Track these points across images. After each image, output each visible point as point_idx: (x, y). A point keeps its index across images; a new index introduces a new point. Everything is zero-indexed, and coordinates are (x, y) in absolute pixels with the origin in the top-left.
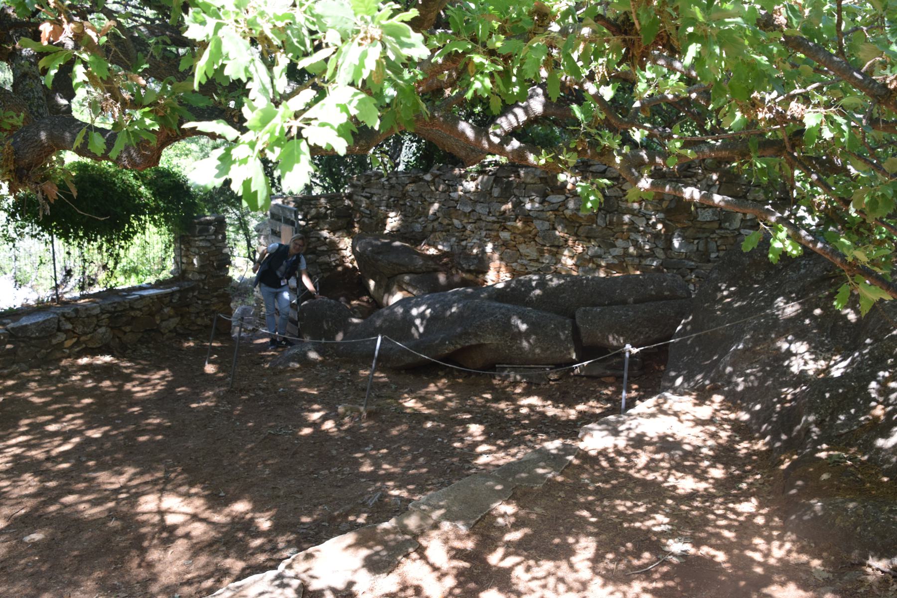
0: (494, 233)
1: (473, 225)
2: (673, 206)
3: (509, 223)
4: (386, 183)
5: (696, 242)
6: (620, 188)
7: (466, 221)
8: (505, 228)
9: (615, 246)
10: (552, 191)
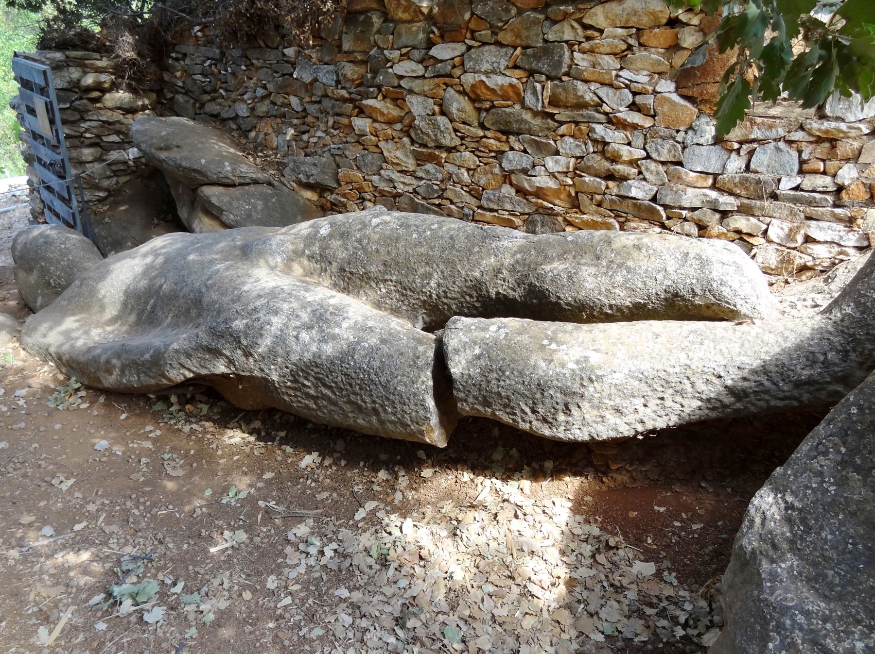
0: (345, 121)
1: (317, 106)
2: (699, 61)
3: (364, 102)
4: (199, 34)
6: (579, 21)
7: (307, 99)
8: (361, 112)
10: (442, 36)
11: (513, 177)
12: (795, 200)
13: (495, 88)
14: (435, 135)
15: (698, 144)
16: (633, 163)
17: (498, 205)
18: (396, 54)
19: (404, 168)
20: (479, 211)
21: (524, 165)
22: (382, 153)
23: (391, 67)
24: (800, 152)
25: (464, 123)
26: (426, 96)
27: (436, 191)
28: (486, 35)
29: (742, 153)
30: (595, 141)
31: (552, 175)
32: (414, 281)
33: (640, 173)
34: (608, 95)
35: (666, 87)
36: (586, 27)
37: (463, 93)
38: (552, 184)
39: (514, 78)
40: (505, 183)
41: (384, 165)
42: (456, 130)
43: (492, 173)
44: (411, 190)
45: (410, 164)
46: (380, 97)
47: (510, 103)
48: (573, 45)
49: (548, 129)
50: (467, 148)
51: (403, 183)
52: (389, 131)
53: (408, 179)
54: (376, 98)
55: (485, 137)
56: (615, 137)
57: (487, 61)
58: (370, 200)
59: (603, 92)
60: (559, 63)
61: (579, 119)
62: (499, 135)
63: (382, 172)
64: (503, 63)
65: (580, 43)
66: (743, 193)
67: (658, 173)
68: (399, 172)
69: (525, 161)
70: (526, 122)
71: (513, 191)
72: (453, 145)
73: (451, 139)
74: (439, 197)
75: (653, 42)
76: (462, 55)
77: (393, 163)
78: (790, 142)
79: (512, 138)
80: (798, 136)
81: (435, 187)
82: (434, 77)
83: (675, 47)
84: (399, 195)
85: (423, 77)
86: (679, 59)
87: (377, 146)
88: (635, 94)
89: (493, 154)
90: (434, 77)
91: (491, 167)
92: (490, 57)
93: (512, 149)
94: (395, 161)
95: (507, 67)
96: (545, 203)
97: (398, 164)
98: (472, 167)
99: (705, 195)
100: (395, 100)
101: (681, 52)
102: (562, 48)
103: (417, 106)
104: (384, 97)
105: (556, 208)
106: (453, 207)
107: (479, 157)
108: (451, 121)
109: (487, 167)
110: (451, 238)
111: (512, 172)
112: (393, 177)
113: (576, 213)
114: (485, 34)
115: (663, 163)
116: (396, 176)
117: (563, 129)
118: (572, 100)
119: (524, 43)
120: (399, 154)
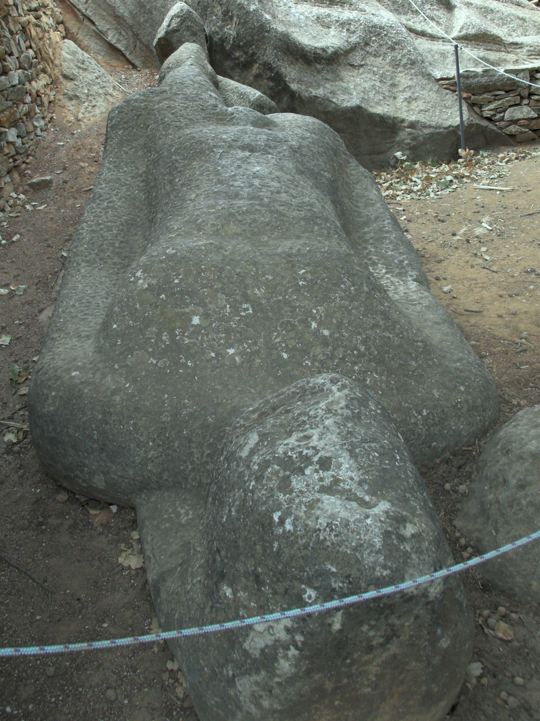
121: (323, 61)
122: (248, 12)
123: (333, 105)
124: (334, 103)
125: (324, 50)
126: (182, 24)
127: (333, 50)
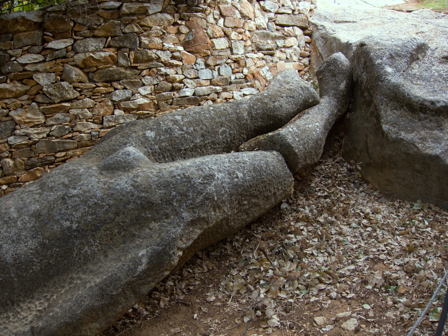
2: (191, 38)
5: (217, 68)
9: (144, 85)
11: (122, 105)
12: (236, 83)
13: (100, 59)
14: (61, 94)
15: (202, 69)
16: (181, 82)
17: (115, 122)
18: (20, 51)
19: (37, 123)
20: (103, 130)
21: (127, 96)
22: (13, 119)
23: (15, 60)
24: (231, 66)
25: (79, 82)
26: (48, 72)
27: (68, 129)
28: (87, 33)
29: (216, 69)
30: (162, 75)
31: (145, 96)
32: (219, 138)
33: (185, 85)
34: (161, 54)
35: (181, 48)
36: (142, 26)
37: (76, 66)
38: (146, 101)
39: (110, 52)
40: (115, 109)
41: (18, 127)
42: (75, 88)
43: (107, 106)
44: (45, 135)
45: (41, 119)
46: (8, 81)
47: (110, 65)
48: (139, 34)
49: (135, 74)
50: (86, 96)
51: (37, 133)
52: (19, 102)
53: (40, 130)
54: (6, 82)
55: (97, 86)
56: (171, 72)
57: (92, 46)
58: (7, 157)
59: (159, 53)
60: (136, 42)
61: (152, 66)
62: (105, 84)
63: (17, 132)
64: (101, 46)
65: (142, 33)
66: (222, 84)
67: (192, 83)
68: (31, 127)
69: (128, 93)
70: (123, 73)
71: (122, 112)
72: (75, 96)
73: (72, 94)
74: (70, 132)
75: (171, 32)
76: (73, 44)
77: (25, 123)
78: (227, 64)
79: (115, 84)
80: (229, 61)
81: (66, 127)
82: (52, 60)
83: (179, 33)
84: (35, 143)
85: (44, 61)
86: (182, 37)
87: (7, 115)
88: (171, 52)
89: (103, 95)
90: (52, 60)
91: (105, 102)
92: (92, 44)
93: (116, 89)
94: (27, 121)
95: (104, 47)
96: (145, 112)
97: (30, 122)
98: (92, 106)
99: (211, 88)
100: (21, 81)
101: (182, 35)
102: (134, 35)
103: (43, 80)
104: (11, 81)
105: (150, 112)
106: (83, 135)
107: (94, 99)
108: (71, 84)
109: (102, 103)
110: (224, 110)
111: (121, 101)
112: (29, 131)
113: (160, 112)
114: (86, 32)
115: (191, 79)
116: (30, 131)
117: (144, 72)
118: (145, 58)
119: (113, 35)
120: (29, 115)
121: (428, 112)
122: (374, 65)
123: (416, 150)
124: (417, 148)
125: (432, 103)
126: (327, 67)
127: (444, 104)
